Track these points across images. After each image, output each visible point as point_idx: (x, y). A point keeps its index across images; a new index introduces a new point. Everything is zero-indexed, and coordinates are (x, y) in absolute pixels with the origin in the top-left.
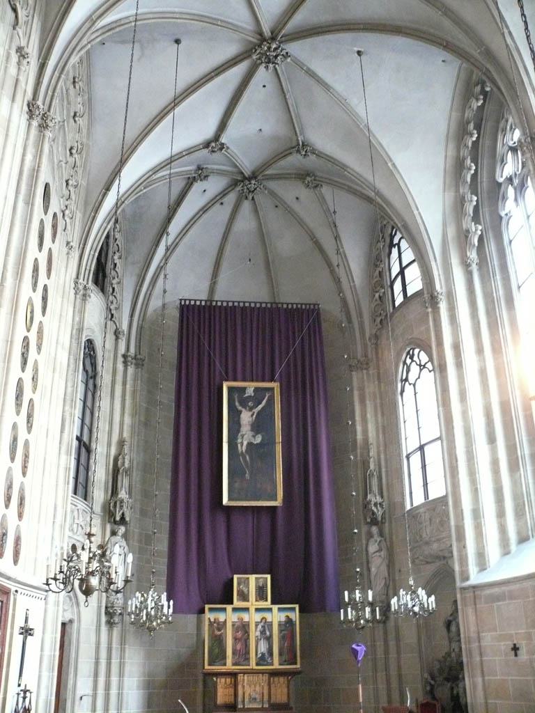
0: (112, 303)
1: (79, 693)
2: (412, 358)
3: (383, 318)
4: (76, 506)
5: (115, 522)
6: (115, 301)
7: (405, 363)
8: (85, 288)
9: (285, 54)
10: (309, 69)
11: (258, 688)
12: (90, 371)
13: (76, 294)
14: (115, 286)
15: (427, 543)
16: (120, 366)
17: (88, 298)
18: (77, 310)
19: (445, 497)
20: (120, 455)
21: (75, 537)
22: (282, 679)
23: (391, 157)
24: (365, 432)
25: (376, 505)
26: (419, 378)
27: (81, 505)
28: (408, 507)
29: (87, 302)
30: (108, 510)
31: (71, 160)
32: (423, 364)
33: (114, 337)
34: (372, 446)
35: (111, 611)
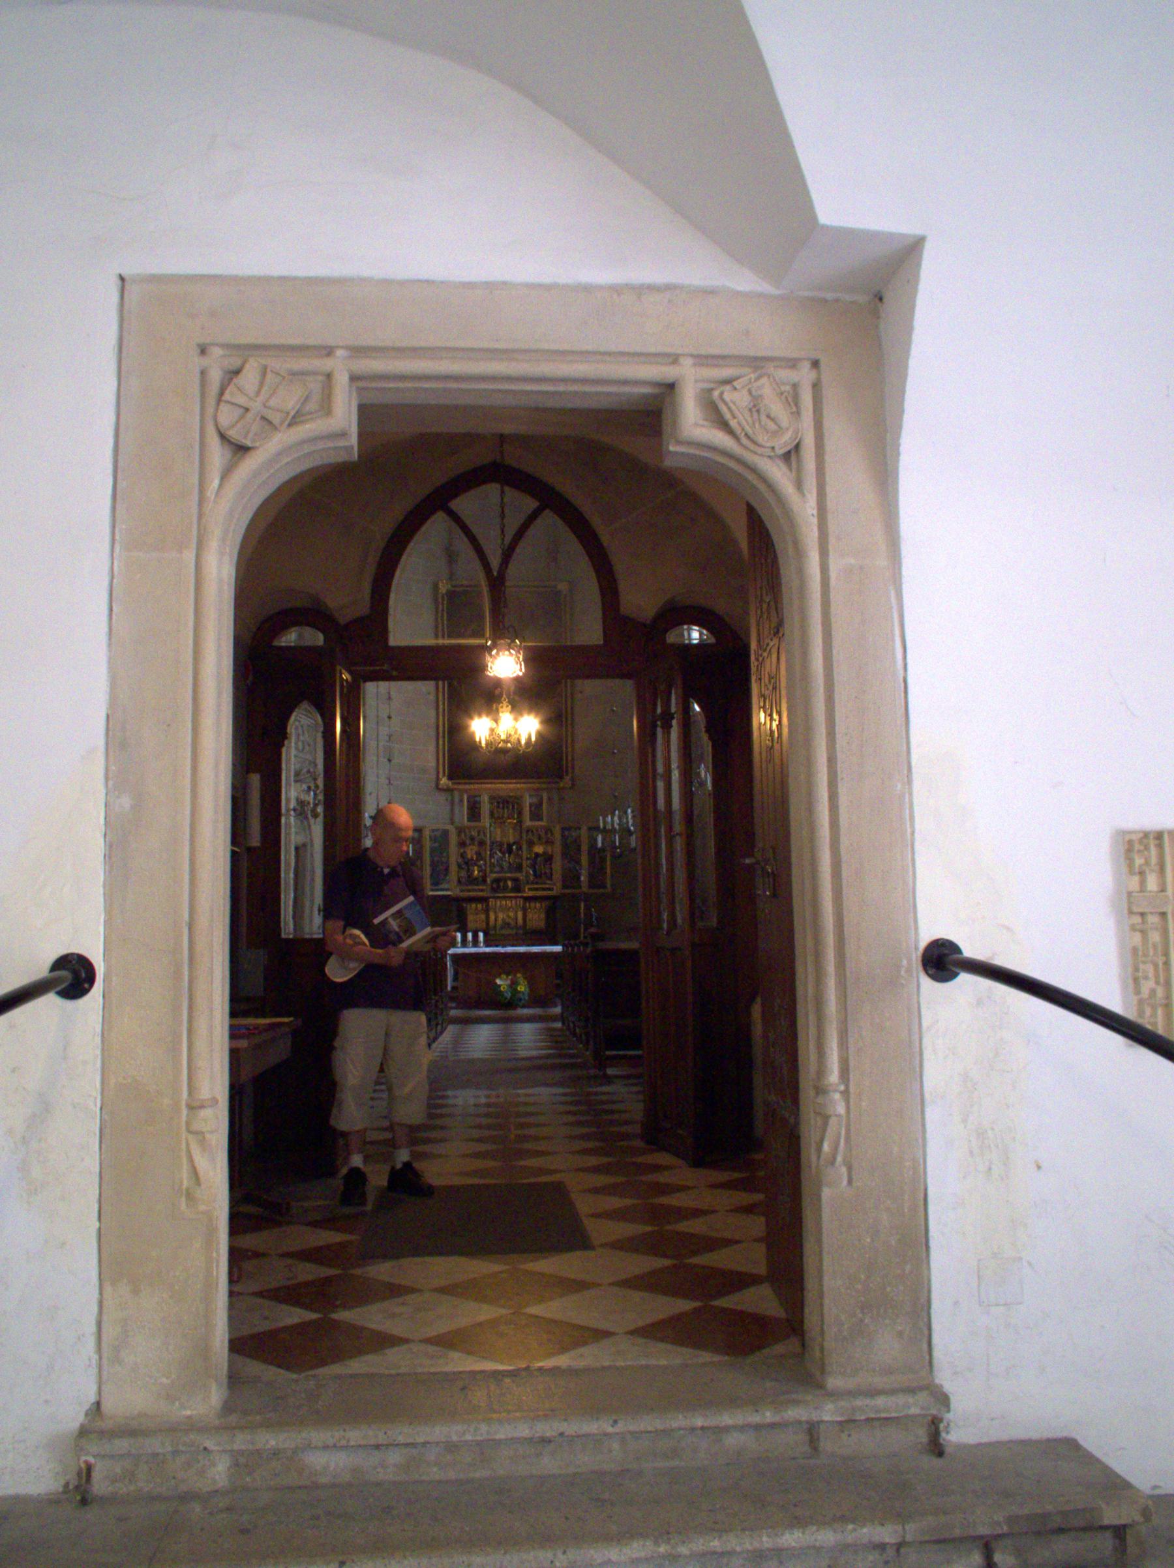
22: (538, 905)
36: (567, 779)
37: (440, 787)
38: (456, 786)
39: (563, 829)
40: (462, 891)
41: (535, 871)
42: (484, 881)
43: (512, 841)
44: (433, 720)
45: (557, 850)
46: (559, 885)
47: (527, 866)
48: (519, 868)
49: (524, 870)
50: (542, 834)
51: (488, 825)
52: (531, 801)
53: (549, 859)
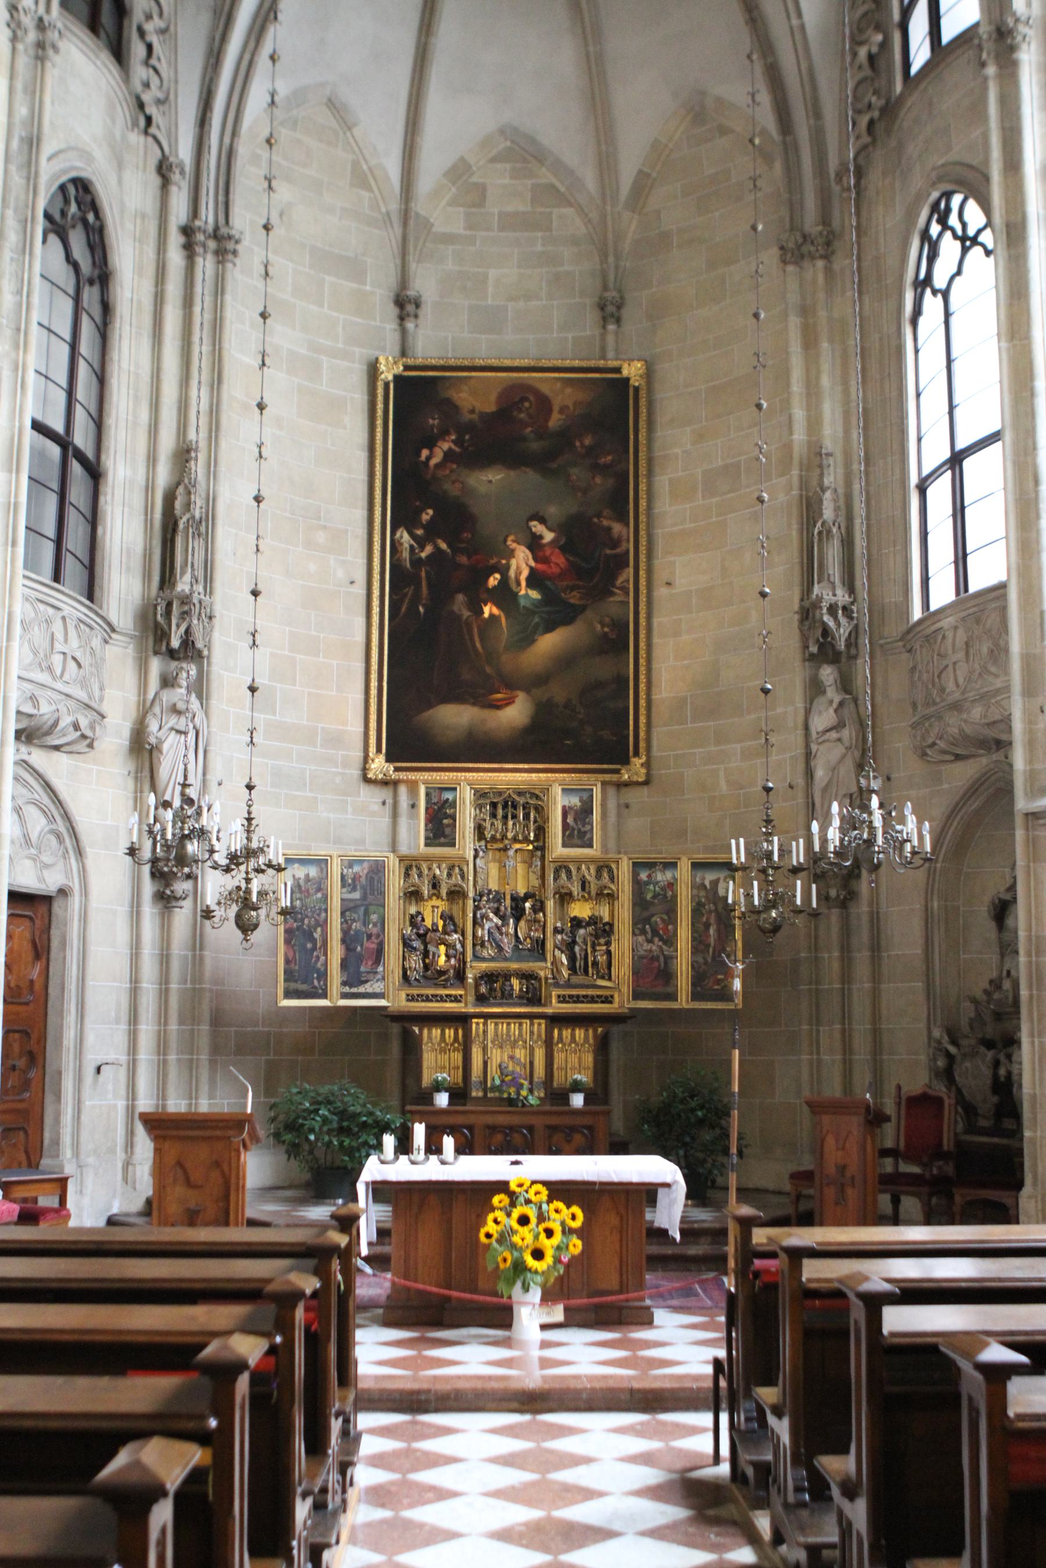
0: (147, 85)
1: (92, 1059)
2: (943, 221)
3: (876, 114)
4: (59, 609)
5: (172, 654)
6: (155, 81)
7: (925, 235)
8: (41, 25)
11: (520, 1054)
12: (86, 267)
13: (14, 39)
14: (154, 39)
15: (956, 707)
16: (175, 257)
17: (50, 52)
18: (19, 86)
19: (1002, 587)
20: (178, 484)
21: (59, 686)
22: (579, 1033)
24: (814, 423)
25: (832, 610)
26: (959, 272)
27: (73, 606)
28: (917, 613)
29: (48, 64)
30: (151, 624)
32: (971, 232)
33: (157, 181)
34: (831, 460)
35: (166, 869)
36: (637, 762)
37: (370, 775)
38: (402, 775)
39: (637, 866)
40: (411, 998)
41: (572, 959)
42: (460, 976)
43: (522, 891)
44: (360, 637)
45: (624, 914)
46: (626, 989)
47: (556, 946)
48: (539, 949)
49: (549, 957)
50: (590, 877)
51: (470, 855)
52: (567, 804)
53: (604, 930)
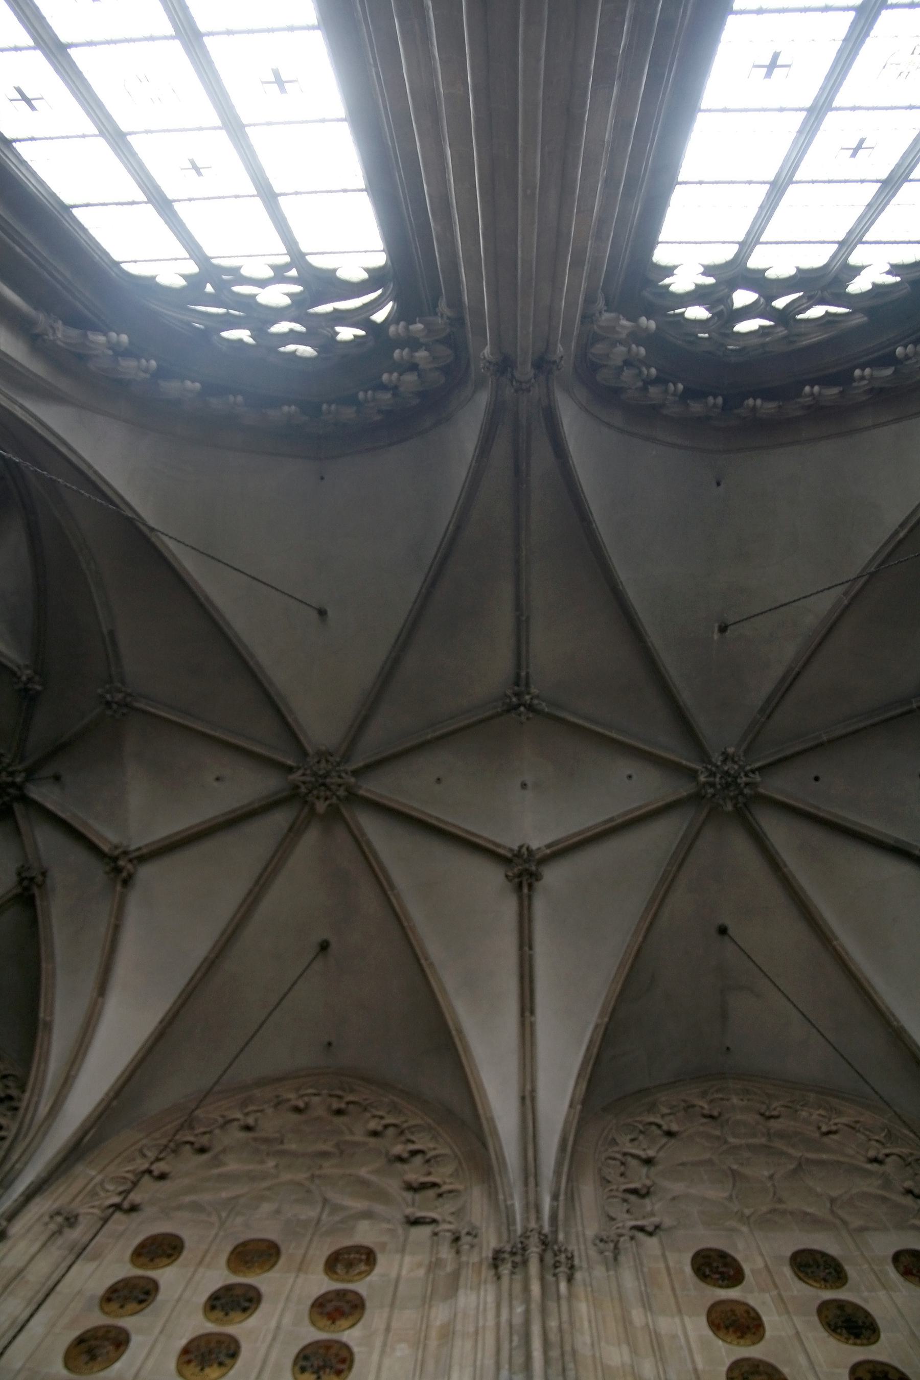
9: (721, 758)
10: (762, 710)
23: (891, 532)
31: (890, 1166)
